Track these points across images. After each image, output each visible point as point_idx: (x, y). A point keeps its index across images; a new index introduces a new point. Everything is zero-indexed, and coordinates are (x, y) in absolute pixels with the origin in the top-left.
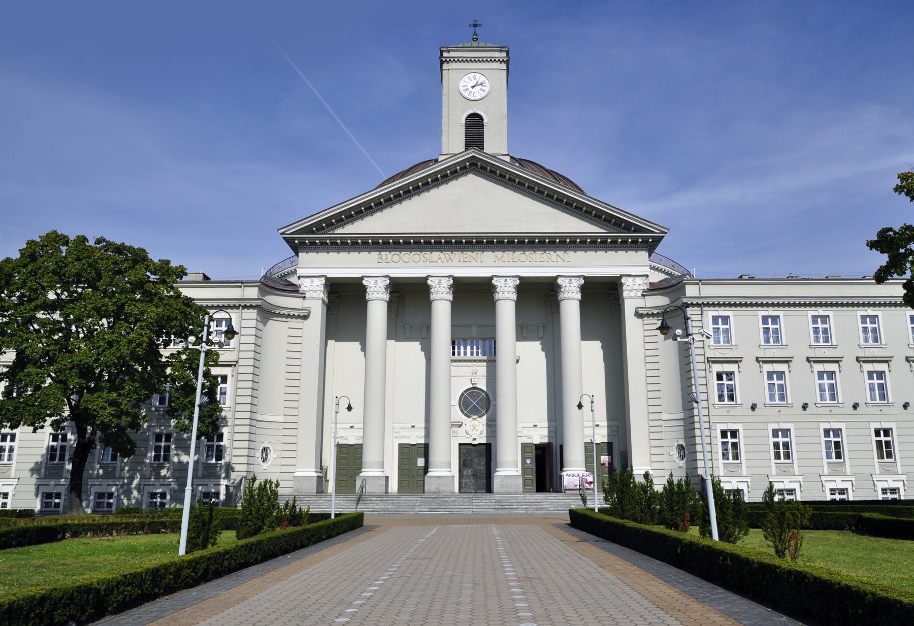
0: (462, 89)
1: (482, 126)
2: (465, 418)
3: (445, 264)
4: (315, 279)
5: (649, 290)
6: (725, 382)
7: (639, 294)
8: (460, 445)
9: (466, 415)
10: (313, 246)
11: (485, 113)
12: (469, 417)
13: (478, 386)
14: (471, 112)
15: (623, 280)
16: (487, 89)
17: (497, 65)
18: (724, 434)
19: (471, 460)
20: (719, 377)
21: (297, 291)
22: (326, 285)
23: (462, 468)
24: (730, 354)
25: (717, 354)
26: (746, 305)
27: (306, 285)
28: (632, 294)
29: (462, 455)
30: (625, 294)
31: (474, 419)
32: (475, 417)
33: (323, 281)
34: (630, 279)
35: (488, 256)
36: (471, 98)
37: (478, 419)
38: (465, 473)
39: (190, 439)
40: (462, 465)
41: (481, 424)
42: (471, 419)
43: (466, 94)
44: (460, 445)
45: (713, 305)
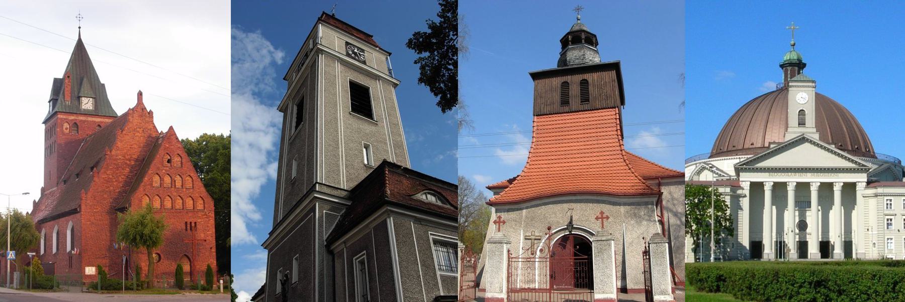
0: (797, 99)
1: (805, 115)
3: (794, 177)
4: (747, 182)
5: (866, 187)
6: (889, 222)
7: (863, 189)
10: (745, 170)
11: (807, 109)
14: (799, 110)
15: (857, 184)
16: (807, 99)
17: (811, 89)
18: (888, 239)
20: (888, 220)
21: (740, 187)
22: (750, 185)
24: (892, 212)
25: (887, 212)
26: (898, 196)
27: (743, 185)
28: (860, 189)
30: (857, 189)
33: (749, 183)
34: (860, 183)
35: (809, 174)
36: (801, 103)
39: (714, 236)
43: (799, 101)
45: (887, 196)
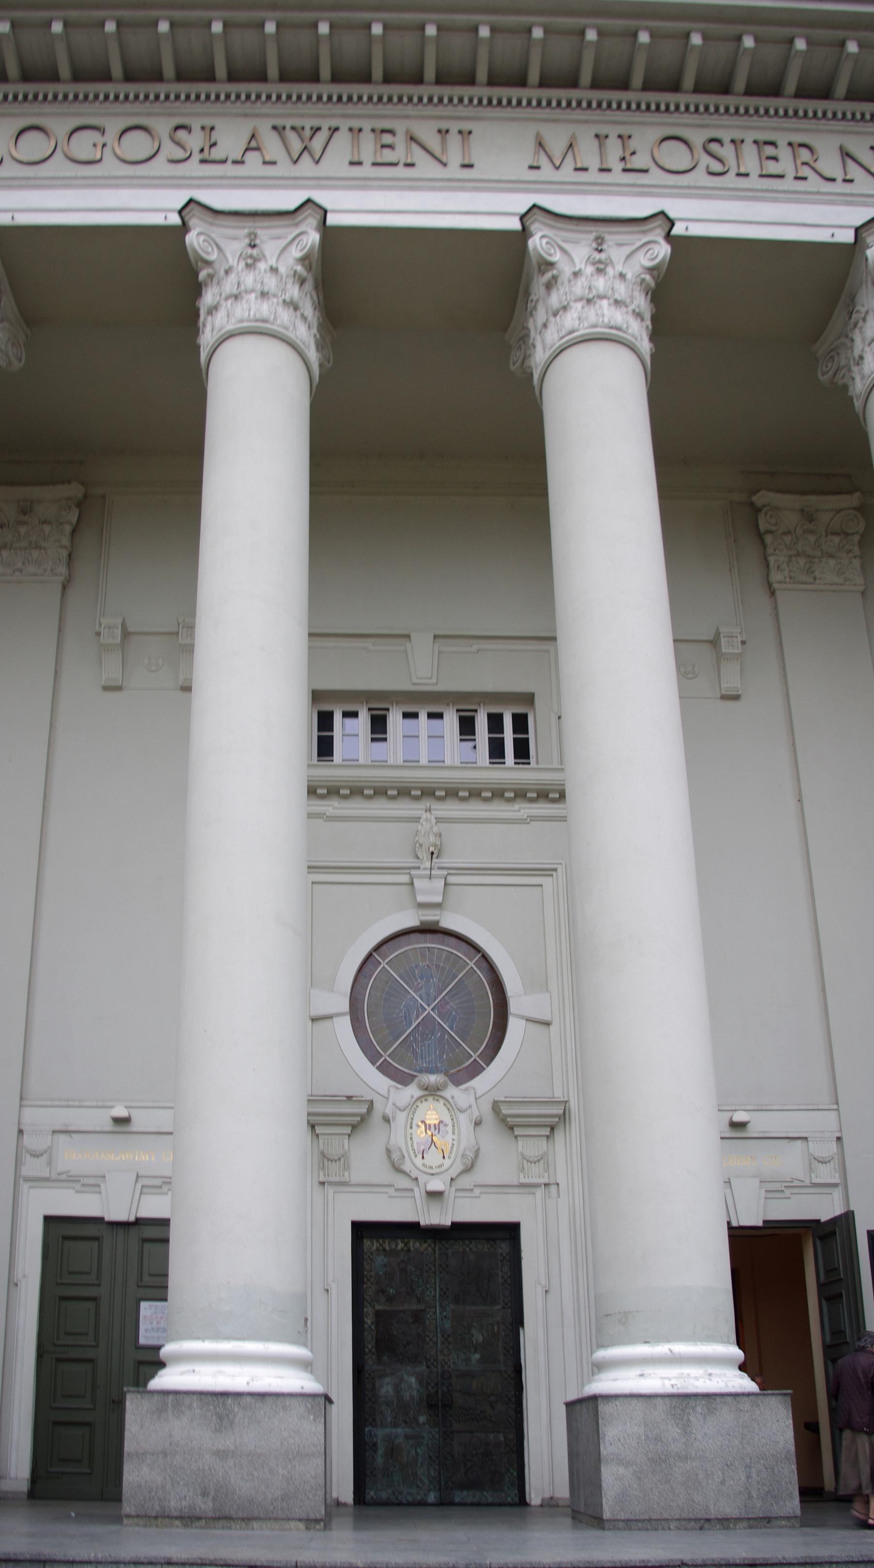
2: (380, 1082)
8: (360, 1230)
9: (385, 1069)
12: (403, 1080)
13: (450, 921)
19: (418, 1317)
23: (370, 1362)
29: (370, 1290)
31: (432, 1092)
32: (433, 1079)
37: (452, 1092)
38: (386, 1388)
40: (370, 1346)
41: (464, 1121)
42: (412, 1091)
44: (360, 1230)
